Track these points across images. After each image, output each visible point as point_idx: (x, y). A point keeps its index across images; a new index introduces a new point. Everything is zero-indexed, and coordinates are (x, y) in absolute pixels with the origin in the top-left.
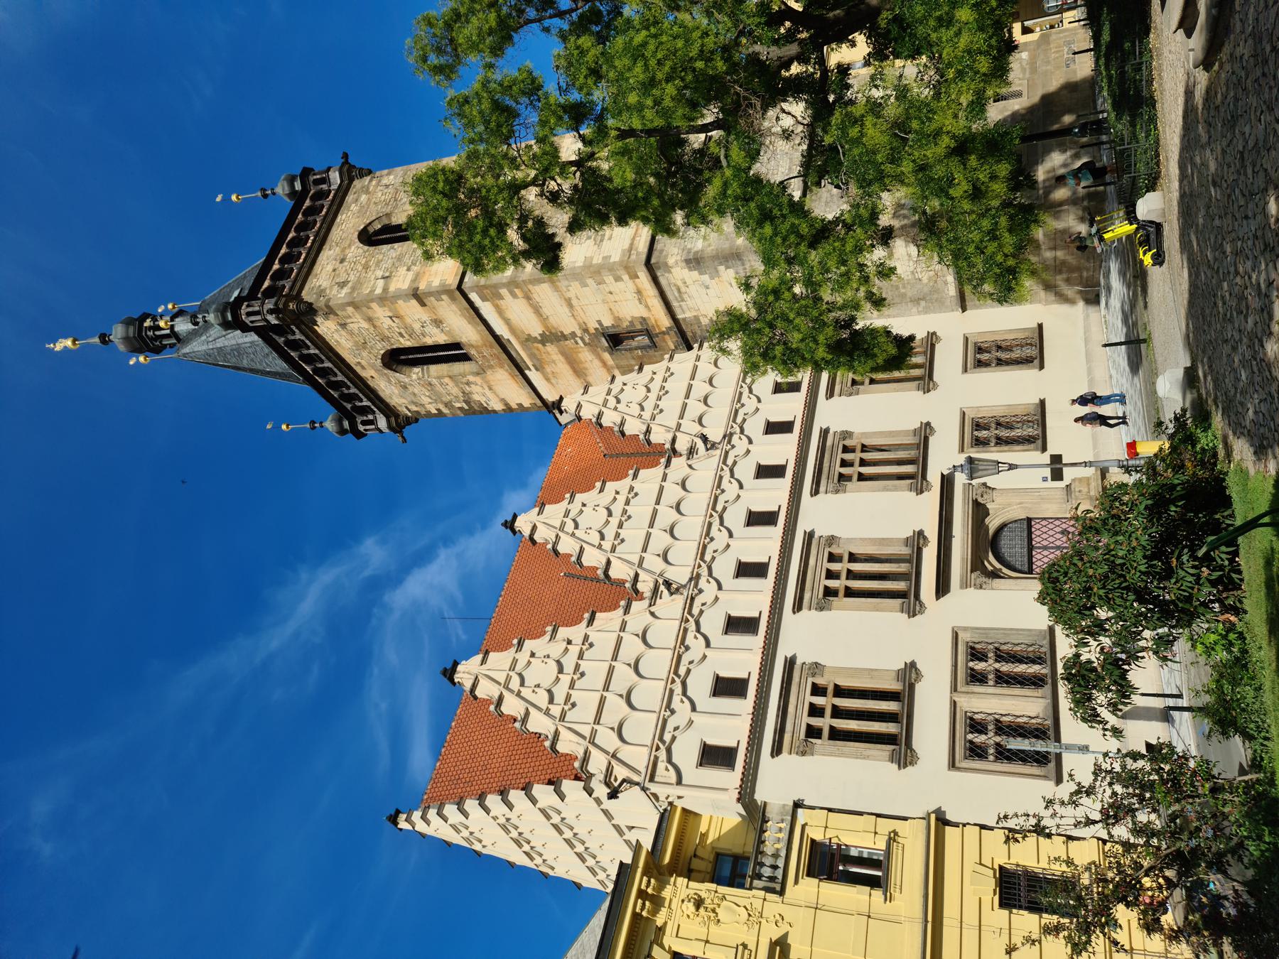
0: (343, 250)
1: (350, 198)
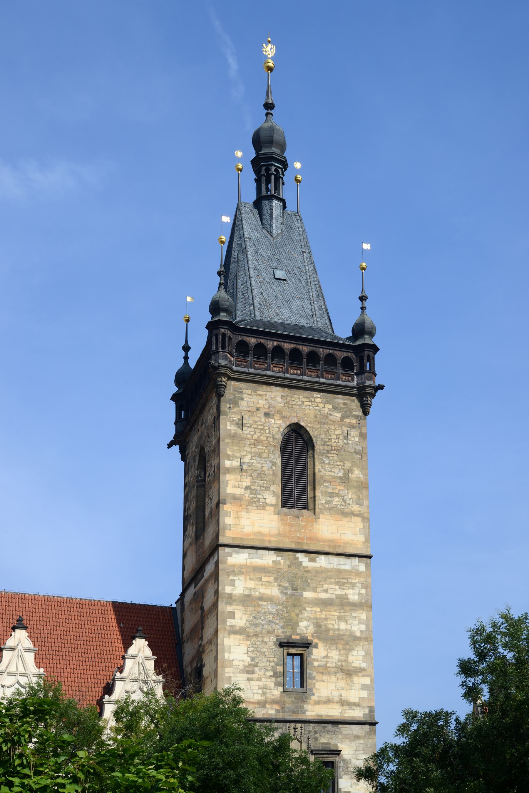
0: (279, 412)
1: (340, 400)
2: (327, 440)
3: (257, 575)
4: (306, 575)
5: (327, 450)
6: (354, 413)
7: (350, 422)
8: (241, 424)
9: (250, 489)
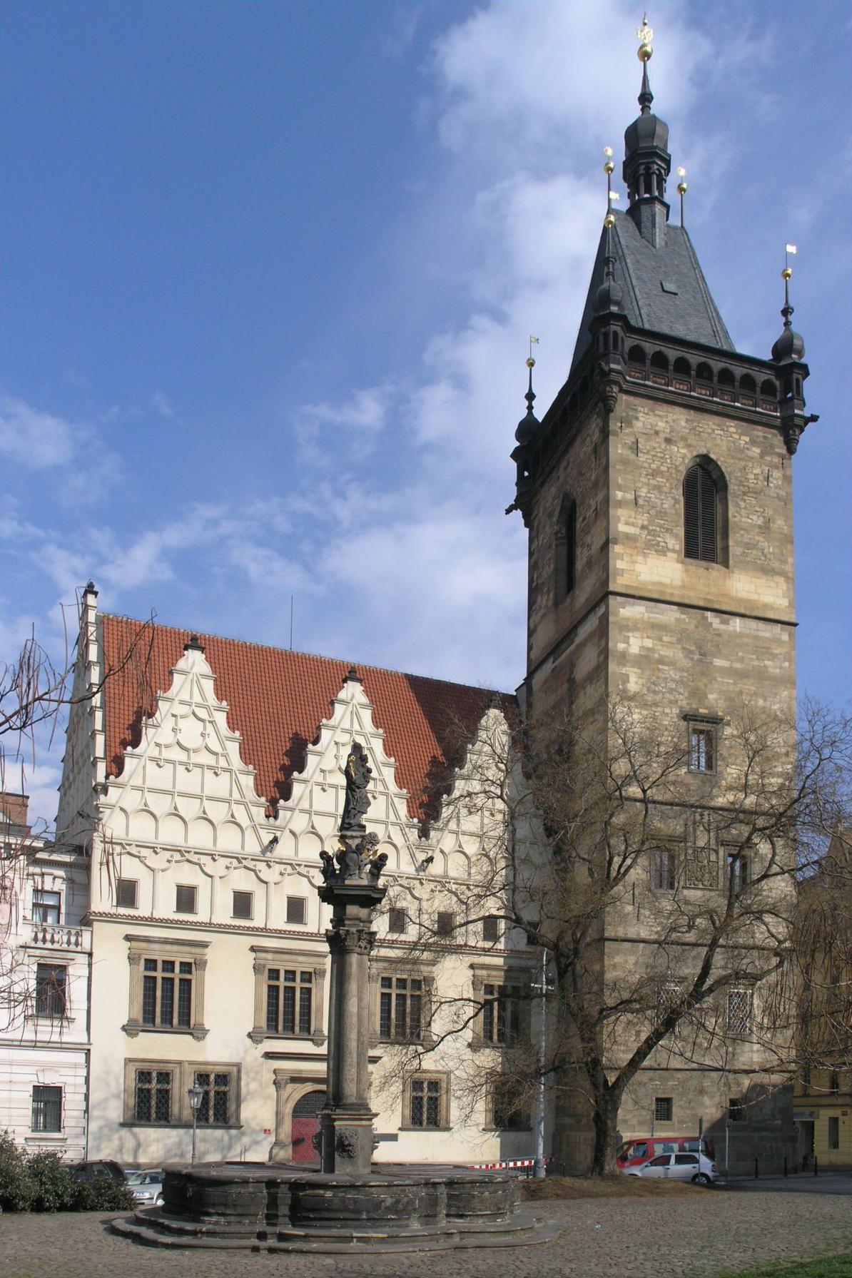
0: (684, 439)
1: (759, 432)
2: (743, 479)
3: (656, 632)
4: (716, 638)
5: (743, 492)
6: (777, 450)
7: (771, 461)
8: (635, 448)
9: (648, 529)
